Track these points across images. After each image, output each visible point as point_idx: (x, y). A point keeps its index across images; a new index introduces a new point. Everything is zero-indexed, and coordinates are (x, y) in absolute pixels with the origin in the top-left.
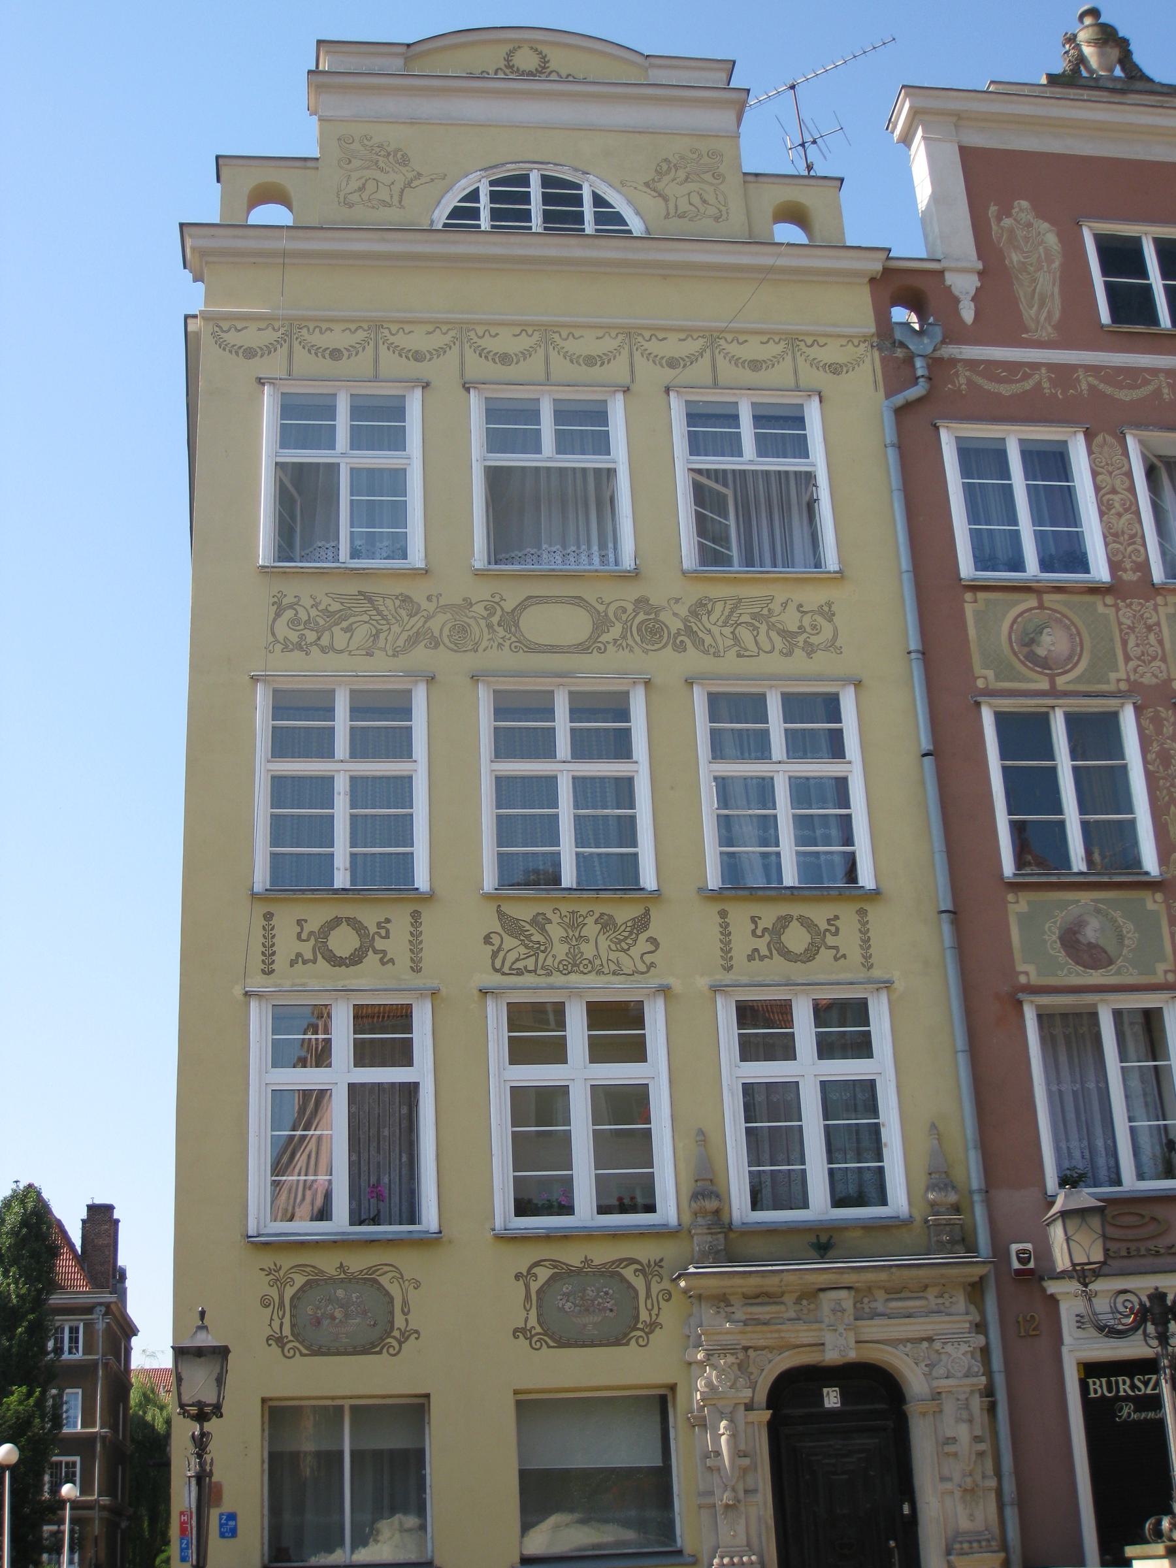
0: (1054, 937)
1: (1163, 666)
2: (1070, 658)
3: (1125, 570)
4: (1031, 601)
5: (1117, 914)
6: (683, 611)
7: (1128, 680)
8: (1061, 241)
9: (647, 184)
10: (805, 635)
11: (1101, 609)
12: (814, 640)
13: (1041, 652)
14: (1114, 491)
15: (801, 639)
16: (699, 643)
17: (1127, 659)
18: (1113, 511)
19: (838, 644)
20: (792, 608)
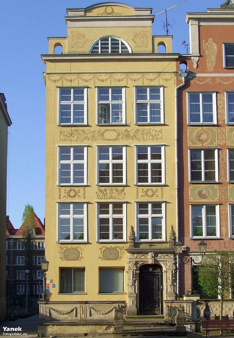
0: (197, 193)
1: (225, 141)
2: (207, 139)
3: (220, 121)
4: (200, 128)
5: (209, 189)
6: (134, 132)
7: (217, 144)
8: (217, 48)
9: (132, 40)
10: (156, 136)
11: (214, 130)
12: (158, 137)
13: (201, 139)
14: (220, 105)
15: (155, 137)
16: (136, 138)
17: (218, 140)
18: (220, 109)
19: (162, 138)
20: (154, 131)
